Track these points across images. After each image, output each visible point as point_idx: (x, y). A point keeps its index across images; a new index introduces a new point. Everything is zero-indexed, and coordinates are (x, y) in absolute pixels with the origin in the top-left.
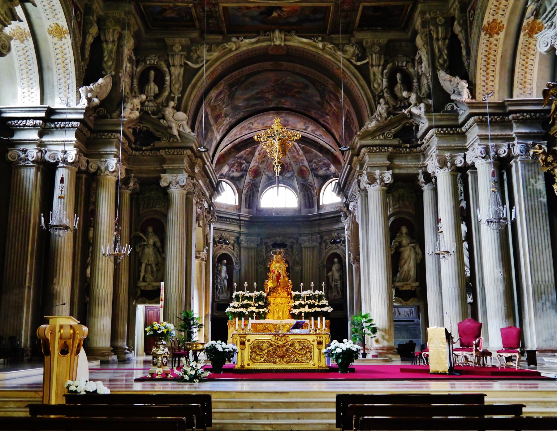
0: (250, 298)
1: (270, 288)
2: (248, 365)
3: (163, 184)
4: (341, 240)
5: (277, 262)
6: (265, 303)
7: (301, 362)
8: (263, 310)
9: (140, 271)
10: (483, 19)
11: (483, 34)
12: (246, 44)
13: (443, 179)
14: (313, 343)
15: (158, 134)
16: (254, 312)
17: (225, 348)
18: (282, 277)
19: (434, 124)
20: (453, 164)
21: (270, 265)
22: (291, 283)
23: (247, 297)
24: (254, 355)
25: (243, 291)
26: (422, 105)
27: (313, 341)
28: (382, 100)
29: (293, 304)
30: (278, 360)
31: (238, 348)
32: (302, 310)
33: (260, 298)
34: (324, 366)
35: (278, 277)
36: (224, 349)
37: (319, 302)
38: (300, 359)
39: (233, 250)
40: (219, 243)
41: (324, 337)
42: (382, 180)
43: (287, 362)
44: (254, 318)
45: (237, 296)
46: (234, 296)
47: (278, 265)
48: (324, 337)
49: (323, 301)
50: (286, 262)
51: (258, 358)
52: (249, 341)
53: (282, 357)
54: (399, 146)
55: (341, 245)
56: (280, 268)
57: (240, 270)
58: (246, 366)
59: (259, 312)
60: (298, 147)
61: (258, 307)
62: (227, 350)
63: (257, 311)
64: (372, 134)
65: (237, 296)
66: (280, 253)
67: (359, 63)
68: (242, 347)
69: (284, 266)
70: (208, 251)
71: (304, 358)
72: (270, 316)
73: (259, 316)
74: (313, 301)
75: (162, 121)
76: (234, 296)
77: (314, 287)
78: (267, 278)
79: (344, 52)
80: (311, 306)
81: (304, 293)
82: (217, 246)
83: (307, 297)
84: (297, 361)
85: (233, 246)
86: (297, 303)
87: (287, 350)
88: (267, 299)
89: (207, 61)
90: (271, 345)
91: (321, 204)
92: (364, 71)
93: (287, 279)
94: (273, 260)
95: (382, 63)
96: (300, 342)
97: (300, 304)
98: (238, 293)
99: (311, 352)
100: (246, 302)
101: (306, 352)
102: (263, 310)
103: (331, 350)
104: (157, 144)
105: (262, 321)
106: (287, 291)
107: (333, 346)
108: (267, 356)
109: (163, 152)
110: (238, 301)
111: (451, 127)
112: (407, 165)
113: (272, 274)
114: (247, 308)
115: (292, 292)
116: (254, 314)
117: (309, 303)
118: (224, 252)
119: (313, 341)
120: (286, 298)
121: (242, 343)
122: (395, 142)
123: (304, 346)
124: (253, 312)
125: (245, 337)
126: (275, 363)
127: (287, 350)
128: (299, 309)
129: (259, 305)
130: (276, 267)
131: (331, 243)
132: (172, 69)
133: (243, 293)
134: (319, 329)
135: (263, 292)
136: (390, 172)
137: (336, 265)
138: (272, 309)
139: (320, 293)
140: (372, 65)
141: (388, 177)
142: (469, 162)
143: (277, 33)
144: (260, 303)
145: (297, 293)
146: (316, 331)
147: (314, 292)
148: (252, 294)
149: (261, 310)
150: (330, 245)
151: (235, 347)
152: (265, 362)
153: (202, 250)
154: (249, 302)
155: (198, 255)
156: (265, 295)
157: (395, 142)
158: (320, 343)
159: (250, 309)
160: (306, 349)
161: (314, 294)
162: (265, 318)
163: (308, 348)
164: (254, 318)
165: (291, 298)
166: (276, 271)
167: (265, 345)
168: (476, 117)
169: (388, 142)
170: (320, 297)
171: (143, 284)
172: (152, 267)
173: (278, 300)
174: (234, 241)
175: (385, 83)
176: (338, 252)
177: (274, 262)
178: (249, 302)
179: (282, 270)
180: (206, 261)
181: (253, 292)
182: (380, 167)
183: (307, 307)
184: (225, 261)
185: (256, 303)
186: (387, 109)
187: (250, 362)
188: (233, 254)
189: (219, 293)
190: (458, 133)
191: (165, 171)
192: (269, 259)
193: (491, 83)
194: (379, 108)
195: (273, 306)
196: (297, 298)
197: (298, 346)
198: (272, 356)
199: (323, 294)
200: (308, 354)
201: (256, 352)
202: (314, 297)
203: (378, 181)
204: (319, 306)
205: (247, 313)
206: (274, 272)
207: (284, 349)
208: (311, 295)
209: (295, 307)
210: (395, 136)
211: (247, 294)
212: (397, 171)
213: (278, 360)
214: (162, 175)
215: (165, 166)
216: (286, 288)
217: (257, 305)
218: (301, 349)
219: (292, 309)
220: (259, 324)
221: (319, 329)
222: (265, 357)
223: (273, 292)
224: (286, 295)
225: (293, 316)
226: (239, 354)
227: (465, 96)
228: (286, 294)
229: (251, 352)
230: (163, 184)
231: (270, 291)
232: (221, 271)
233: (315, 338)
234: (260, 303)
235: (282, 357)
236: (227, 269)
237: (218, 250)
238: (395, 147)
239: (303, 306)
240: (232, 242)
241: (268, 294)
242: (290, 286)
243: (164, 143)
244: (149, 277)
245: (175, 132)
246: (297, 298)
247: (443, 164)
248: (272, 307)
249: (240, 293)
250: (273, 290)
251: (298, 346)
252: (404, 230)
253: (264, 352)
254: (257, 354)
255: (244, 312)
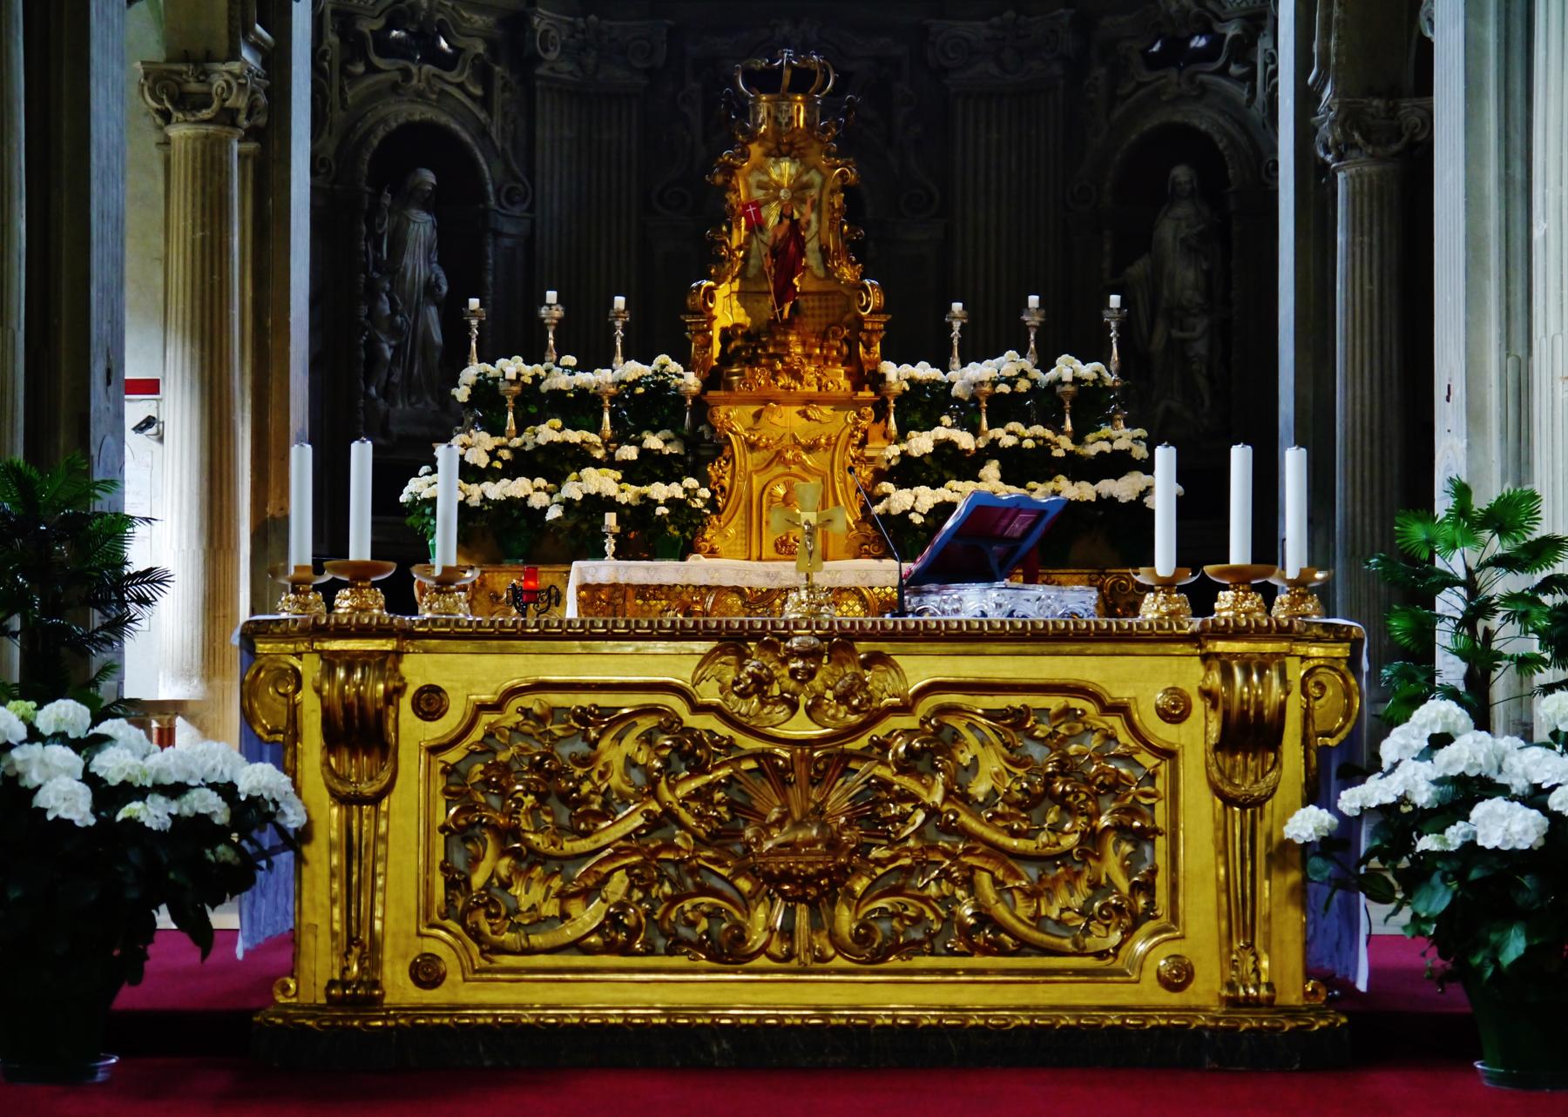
0: (580, 408)
1: (726, 336)
2: (426, 972)
4: (1216, 41)
5: (782, 147)
6: (692, 442)
7: (1025, 947)
8: (676, 491)
14: (1164, 733)
16: (610, 504)
17: (130, 791)
18: (812, 259)
21: (730, 170)
22: (875, 299)
23: (557, 394)
24: (490, 865)
25: (533, 355)
27: (1175, 713)
29: (894, 450)
30: (762, 921)
31: (304, 794)
32: (959, 492)
33: (647, 406)
34: (1292, 996)
35: (787, 253)
36: (107, 795)
37: (1078, 439)
38: (1015, 914)
39: (485, 102)
40: (387, 49)
41: (1296, 671)
43: (871, 950)
44: (610, 546)
45: (486, 391)
46: (462, 394)
47: (784, 171)
48: (1296, 671)
49: (1106, 430)
50: (847, 146)
51: (529, 895)
52: (430, 703)
53: (816, 890)
55: (1223, 72)
56: (799, 189)
57: (530, 241)
58: (399, 988)
59: (649, 503)
61: (633, 473)
62: (152, 813)
63: (628, 495)
65: (486, 391)
66: (803, 81)
68: (359, 771)
69: (832, 174)
70: (277, 61)
71: (1064, 902)
72: (725, 532)
73: (648, 534)
74: (1038, 429)
76: (462, 394)
77: (1041, 330)
78: (707, 259)
80: (1019, 466)
81: (967, 376)
82: (372, 69)
83: (995, 399)
84: (986, 935)
85: (483, 75)
86: (921, 443)
87: (872, 812)
88: (702, 407)
90: (690, 752)
93: (848, 273)
94: (752, 136)
96: (1017, 719)
97: (944, 447)
98: (492, 371)
99: (1144, 836)
100: (548, 432)
101: (1092, 840)
102: (676, 491)
103: (1398, 822)
105: (665, 572)
106: (850, 360)
107: (1405, 773)
108: (639, 880)
110: (496, 429)
113: (738, 236)
114: (557, 479)
115: (890, 370)
116: (611, 519)
117: (1008, 441)
118: (421, 113)
119: (1175, 713)
120: (840, 404)
121: (359, 732)
123: (1066, 767)
124: (597, 504)
125: (385, 664)
126: (729, 951)
127: (872, 812)
128: (936, 484)
129: (645, 454)
130: (772, 188)
131: (1154, 63)
133: (528, 371)
134: (1240, 578)
135: (675, 367)
137: (1183, 210)
138: (741, 485)
139: (1088, 370)
144: (653, 442)
145: (924, 371)
146: (1202, 597)
147: (1046, 364)
148: (601, 377)
149: (659, 491)
150: (1147, 76)
151: (257, 778)
152: (616, 937)
153: (222, 45)
154: (574, 437)
155: (193, 86)
156: (692, 381)
158: (1249, 734)
159: (572, 490)
160: (1086, 793)
161: (1044, 378)
162: (683, 550)
163: (1115, 786)
164: (610, 546)
165: (881, 414)
166: (772, 216)
167: (613, 753)
170: (1089, 406)
173: (786, 420)
174: (491, 44)
176: (1203, 119)
177: (755, 149)
178: (574, 437)
179: (817, 206)
180: (252, 134)
181: (608, 364)
183: (991, 470)
184: (429, 177)
185: (621, 439)
187: (441, 944)
188: (482, 133)
189: (386, 393)
192: (726, 128)
195: (748, 461)
196: (923, 406)
197: (989, 772)
198: (692, 881)
199: (1110, 379)
200: (1112, 865)
201: (507, 836)
202: (1042, 404)
204: (1079, 469)
205: (554, 513)
206: (756, 226)
207: (838, 799)
208: (1023, 385)
209: (908, 472)
211: (562, 377)
213: (762, 921)
216: (842, 335)
217: (629, 453)
218: (1031, 802)
219: (887, 486)
220: (643, 591)
221: (1240, 578)
222: (618, 885)
223: (752, 361)
224: (845, 384)
225: (892, 535)
226: (322, 858)
228: (839, 378)
229: (460, 834)
231: (726, 359)
232: (398, 244)
233: (1190, 673)
234: (653, 442)
235: (816, 890)
236: (441, 229)
237: (375, 95)
239: (967, 466)
240: (480, 48)
241: (714, 379)
242: (876, 324)
246: (923, 406)
248: (743, 472)
249: (512, 367)
250: (748, 347)
251: (989, 772)
253: (610, 833)
254: (528, 859)
255: (539, 500)
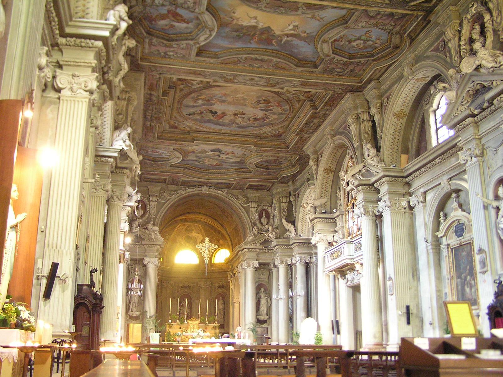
3: (145, 262)
9: (129, 306)
10: (301, 202)
11: (301, 207)
12: (190, 191)
13: (282, 269)
15: (144, 237)
19: (278, 244)
20: (286, 263)
26: (274, 233)
28: (255, 227)
42: (253, 266)
54: (263, 249)
60: (201, 227)
64: (250, 243)
67: (245, 205)
75: (146, 231)
79: (238, 199)
89: (170, 199)
91: (213, 262)
92: (247, 210)
95: (256, 206)
104: (143, 242)
109: (145, 246)
111: (286, 245)
112: (265, 259)
122: (261, 247)
132: (151, 203)
136: (258, 262)
140: (251, 207)
141: (256, 264)
142: (294, 262)
143: (205, 187)
157: (261, 247)
168: (297, 244)
169: (257, 247)
171: (132, 313)
172: (136, 304)
175: (257, 217)
182: (253, 260)
186: (258, 231)
190: (289, 248)
191: (146, 256)
193: (304, 228)
194: (254, 230)
203: (252, 266)
210: (260, 244)
212: (261, 261)
214: (145, 258)
215: (146, 254)
227: (293, 235)
230: (145, 262)
238: (260, 249)
243: (147, 242)
244: (135, 309)
245: (153, 237)
247: (282, 262)
252: (262, 289)
